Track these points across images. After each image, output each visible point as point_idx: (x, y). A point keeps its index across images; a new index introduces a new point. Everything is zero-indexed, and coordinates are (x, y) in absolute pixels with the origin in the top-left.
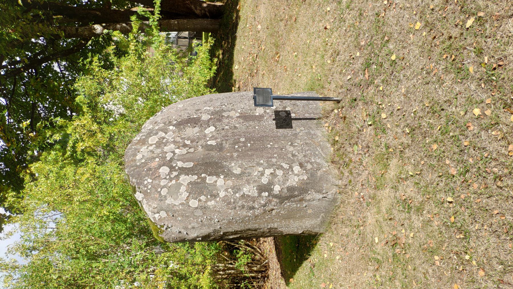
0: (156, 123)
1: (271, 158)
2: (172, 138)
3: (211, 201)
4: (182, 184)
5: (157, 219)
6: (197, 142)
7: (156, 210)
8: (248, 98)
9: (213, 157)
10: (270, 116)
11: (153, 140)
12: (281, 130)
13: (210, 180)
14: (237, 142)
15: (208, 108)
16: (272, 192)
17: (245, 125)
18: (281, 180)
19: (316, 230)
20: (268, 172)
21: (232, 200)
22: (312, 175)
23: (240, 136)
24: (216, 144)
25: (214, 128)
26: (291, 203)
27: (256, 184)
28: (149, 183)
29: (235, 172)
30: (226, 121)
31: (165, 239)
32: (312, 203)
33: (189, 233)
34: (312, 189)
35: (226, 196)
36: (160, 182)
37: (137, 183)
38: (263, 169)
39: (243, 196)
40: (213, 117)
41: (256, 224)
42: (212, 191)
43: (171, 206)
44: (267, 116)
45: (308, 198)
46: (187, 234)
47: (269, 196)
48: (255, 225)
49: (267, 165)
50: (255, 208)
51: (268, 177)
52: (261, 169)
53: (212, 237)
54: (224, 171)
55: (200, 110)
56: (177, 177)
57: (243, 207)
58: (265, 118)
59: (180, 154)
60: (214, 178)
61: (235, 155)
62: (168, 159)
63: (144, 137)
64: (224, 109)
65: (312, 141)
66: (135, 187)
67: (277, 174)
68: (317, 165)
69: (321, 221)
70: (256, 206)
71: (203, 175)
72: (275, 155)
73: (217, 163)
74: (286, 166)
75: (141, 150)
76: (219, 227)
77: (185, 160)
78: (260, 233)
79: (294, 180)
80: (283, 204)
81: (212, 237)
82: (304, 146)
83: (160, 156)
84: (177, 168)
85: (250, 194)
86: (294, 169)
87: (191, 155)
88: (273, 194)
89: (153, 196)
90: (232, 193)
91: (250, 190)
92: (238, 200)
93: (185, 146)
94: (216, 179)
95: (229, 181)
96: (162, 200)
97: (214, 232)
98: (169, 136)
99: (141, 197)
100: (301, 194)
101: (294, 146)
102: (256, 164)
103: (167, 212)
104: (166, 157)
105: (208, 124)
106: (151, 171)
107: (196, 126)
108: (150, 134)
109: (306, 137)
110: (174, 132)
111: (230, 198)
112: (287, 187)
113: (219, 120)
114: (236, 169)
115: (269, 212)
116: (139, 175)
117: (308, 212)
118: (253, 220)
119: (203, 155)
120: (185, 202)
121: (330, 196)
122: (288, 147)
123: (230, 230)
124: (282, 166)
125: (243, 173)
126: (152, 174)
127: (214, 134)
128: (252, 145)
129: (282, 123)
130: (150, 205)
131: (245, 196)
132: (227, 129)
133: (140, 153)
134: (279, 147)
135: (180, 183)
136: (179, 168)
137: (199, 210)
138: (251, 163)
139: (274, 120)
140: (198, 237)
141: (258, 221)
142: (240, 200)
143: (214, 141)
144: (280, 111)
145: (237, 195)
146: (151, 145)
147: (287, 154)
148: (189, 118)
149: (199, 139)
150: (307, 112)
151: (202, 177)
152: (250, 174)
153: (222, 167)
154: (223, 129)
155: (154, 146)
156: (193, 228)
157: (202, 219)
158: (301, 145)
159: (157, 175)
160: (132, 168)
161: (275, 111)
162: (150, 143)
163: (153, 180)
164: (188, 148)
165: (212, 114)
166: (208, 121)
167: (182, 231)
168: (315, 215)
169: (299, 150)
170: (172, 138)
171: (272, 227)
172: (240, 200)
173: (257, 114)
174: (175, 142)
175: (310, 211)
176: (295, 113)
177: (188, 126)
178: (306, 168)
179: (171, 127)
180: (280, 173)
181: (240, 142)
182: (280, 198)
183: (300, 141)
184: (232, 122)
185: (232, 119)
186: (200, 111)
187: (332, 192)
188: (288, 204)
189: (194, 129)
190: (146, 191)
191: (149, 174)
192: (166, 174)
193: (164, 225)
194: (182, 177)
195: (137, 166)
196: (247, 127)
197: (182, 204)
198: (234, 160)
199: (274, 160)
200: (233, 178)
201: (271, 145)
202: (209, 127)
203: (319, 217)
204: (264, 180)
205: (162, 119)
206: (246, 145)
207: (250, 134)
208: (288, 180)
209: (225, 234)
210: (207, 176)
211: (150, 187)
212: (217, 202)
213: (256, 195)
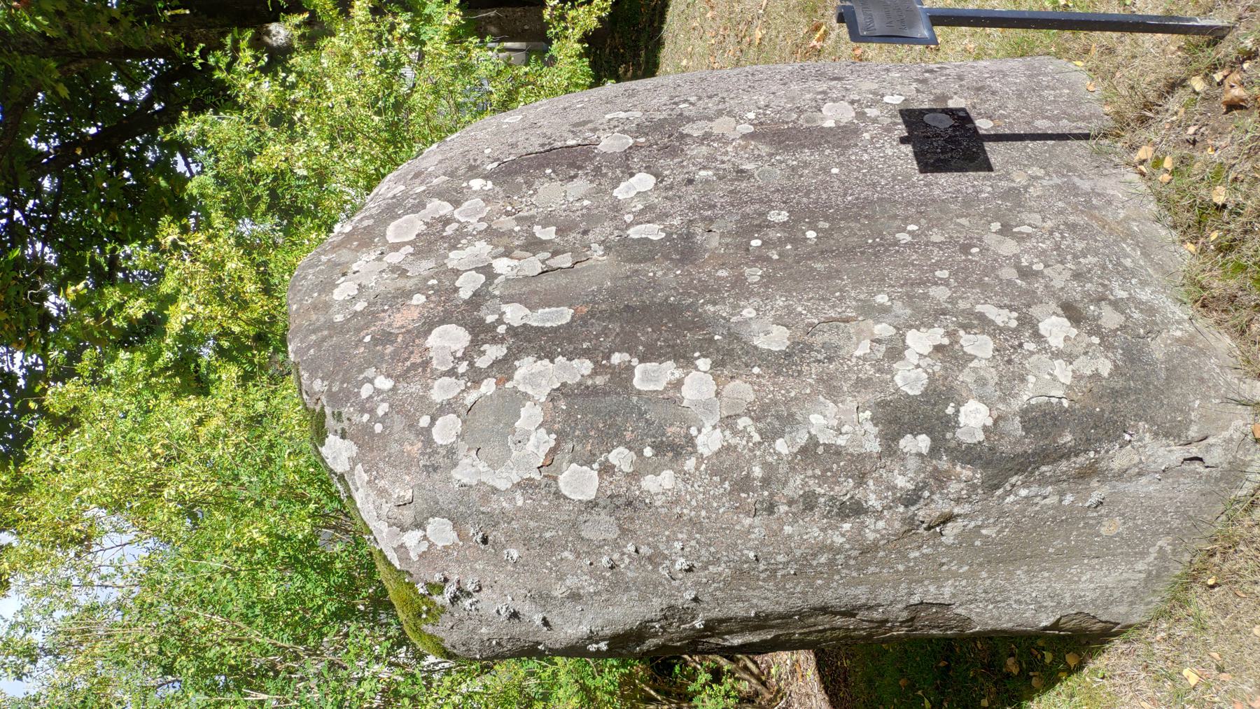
0: (417, 176)
1: (922, 283)
2: (480, 220)
3: (656, 472)
4: (526, 396)
5: (414, 556)
6: (585, 232)
7: (408, 515)
8: (778, 77)
9: (655, 284)
10: (888, 130)
11: (405, 229)
12: (945, 180)
13: (646, 377)
14: (762, 226)
15: (622, 115)
16: (949, 435)
18: (992, 376)
19: (1117, 613)
20: (920, 342)
21: (757, 472)
23: (767, 202)
24: (663, 235)
25: (651, 180)
26: (1035, 489)
27: (869, 397)
28: (378, 392)
29: (760, 342)
31: (447, 645)
32: (1130, 487)
33: (554, 619)
34: (1139, 417)
35: (727, 449)
36: (428, 388)
37: (331, 396)
38: (892, 331)
39: (809, 451)
40: (642, 140)
41: (860, 583)
42: (660, 426)
43: (474, 496)
44: (874, 129)
45: (1116, 465)
46: (546, 622)
47: (934, 451)
48: (853, 591)
49: (909, 311)
50: (866, 512)
51: (923, 363)
52: (883, 329)
53: (655, 641)
54: (711, 340)
55: (591, 121)
56: (504, 368)
57: (809, 502)
58: (867, 136)
59: (512, 275)
60: (669, 370)
61: (754, 274)
62: (465, 294)
63: (366, 223)
64: (686, 114)
65: (1092, 217)
66: (322, 415)
67: (968, 350)
68: (1141, 311)
69: (1149, 573)
70: (873, 501)
71: (617, 358)
72: (942, 274)
73: (674, 311)
74: (1001, 317)
75: (355, 267)
76: (689, 595)
77: (536, 299)
78: (865, 625)
79: (1054, 379)
80: (1000, 492)
81: (655, 641)
82: (1063, 237)
83: (432, 287)
84: (501, 329)
85: (841, 441)
86: (1043, 328)
87: (563, 280)
88: (953, 444)
89: (394, 448)
90: (757, 438)
91: (841, 424)
92: (783, 468)
93: (534, 245)
94: (678, 373)
96: (435, 469)
97: (665, 618)
98: (470, 214)
99: (345, 456)
100: (1087, 443)
101: (1021, 238)
102: (856, 309)
103: (457, 522)
104: (456, 290)
105: (624, 165)
106: (392, 342)
107: (575, 176)
108: (391, 211)
109: (1060, 204)
110: (487, 198)
111: (748, 462)
112: (1024, 413)
113: (670, 151)
114: (767, 333)
115: (929, 528)
116: (338, 362)
117: (1103, 530)
118: (846, 566)
119: (614, 278)
120: (538, 477)
121: (1216, 456)
123: (738, 610)
124: (982, 317)
126: (395, 355)
127: (654, 199)
128: (824, 235)
130: (382, 492)
131: (820, 450)
132: (707, 181)
133: (350, 275)
134: (951, 241)
135: (515, 390)
136: (510, 328)
137: (604, 516)
139: (903, 141)
140: (592, 638)
141: (871, 569)
142: (793, 469)
143: (656, 226)
144: (922, 112)
145: (781, 446)
146: (396, 247)
147: (994, 268)
148: (547, 148)
149: (591, 218)
151: (612, 367)
152: (832, 354)
153: (701, 323)
154: (690, 182)
155: (410, 249)
156: (575, 596)
157: (616, 556)
158: (1051, 233)
160: (313, 337)
161: (901, 112)
162: (391, 237)
164: (547, 255)
165: (640, 130)
166: (627, 154)
167: (525, 608)
168: (1132, 546)
169: (1044, 252)
170: (480, 220)
171: (929, 599)
172: (793, 469)
173: (829, 123)
174: (490, 234)
175: (1111, 527)
176: (990, 118)
177: (545, 176)
178: (1099, 327)
179: (476, 184)
180: (979, 346)
181: (771, 225)
182: (986, 465)
184: (726, 153)
185: (727, 144)
186: (590, 126)
187: (1226, 434)
188: (1023, 492)
189: (570, 185)
190: (367, 430)
191: (382, 355)
192: (453, 354)
193: (446, 580)
194: (526, 367)
195: (331, 326)
196: (793, 169)
197: (526, 485)
198: (752, 294)
200: (756, 370)
201: (910, 233)
202: (632, 175)
203: (1143, 554)
204: (905, 379)
205: (440, 162)
206: (799, 235)
207: (807, 194)
208: (1023, 379)
209: (712, 627)
210: (635, 361)
211: (382, 409)
212: (686, 477)
213: (873, 446)
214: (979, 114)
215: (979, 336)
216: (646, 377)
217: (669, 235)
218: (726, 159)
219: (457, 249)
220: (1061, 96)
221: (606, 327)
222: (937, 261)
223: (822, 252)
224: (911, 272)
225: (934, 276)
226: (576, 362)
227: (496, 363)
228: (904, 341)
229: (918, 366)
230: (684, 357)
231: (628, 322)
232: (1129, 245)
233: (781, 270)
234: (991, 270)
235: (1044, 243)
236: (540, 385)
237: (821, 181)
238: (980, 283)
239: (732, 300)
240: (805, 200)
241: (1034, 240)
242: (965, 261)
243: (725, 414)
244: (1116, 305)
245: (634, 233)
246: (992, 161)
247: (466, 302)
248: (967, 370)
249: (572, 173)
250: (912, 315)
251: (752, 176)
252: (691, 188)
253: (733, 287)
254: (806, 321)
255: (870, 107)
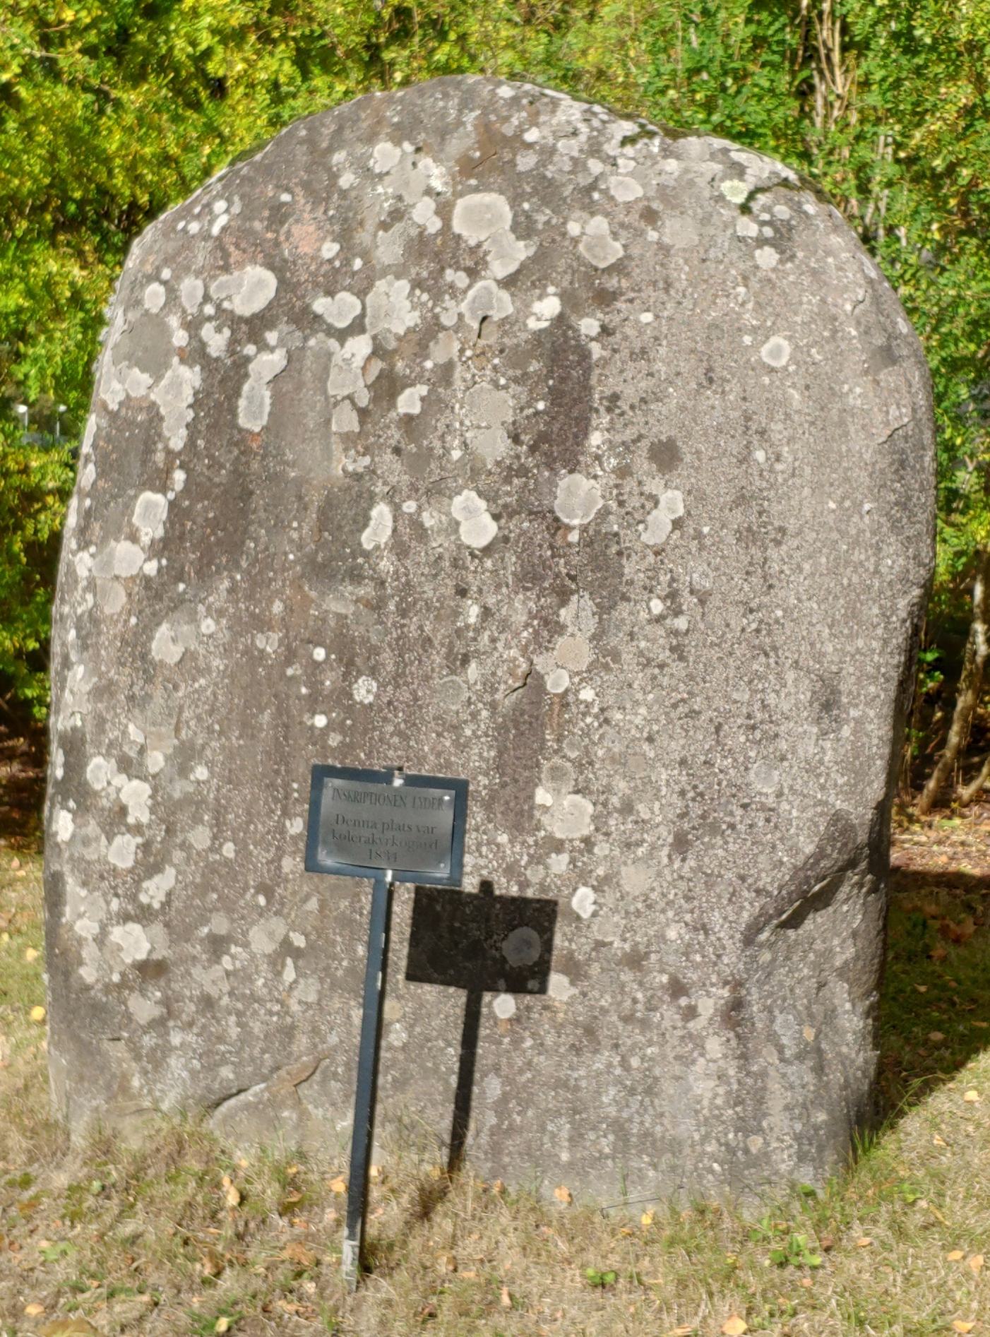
4: (158, 378)
6: (397, 451)
9: (280, 526)
17: (474, 716)
18: (90, 854)
22: (97, 1009)
29: (164, 630)
30: (520, 608)
38: (153, 770)
49: (177, 795)
51: (111, 790)
52: (156, 761)
54: (180, 578)
56: (197, 354)
59: (337, 359)
60: (151, 530)
61: (269, 643)
62: (320, 305)
67: (118, 840)
68: (153, 1050)
71: (179, 476)
72: (229, 850)
73: (234, 547)
74: (155, 890)
77: (288, 387)
79: (80, 916)
82: (271, 1013)
84: (250, 349)
86: (135, 928)
94: (145, 540)
95: (124, 599)
101: (276, 962)
104: (330, 293)
107: (516, 439)
114: (174, 640)
119: (300, 482)
122: (279, 927)
125: (146, 667)
129: (452, 930)
132: (456, 614)
135: (167, 366)
136: (248, 360)
138: (199, 719)
139: (486, 886)
143: (385, 536)
146: (444, 211)
150: (516, 1095)
153: (205, 574)
158: (282, 1003)
159: (235, 255)
163: (218, 238)
169: (250, 979)
173: (542, 796)
174: (430, 330)
176: (516, 1020)
183: (312, 998)
184: (508, 646)
192: (229, 298)
194: (191, 377)
196: (456, 728)
198: (236, 635)
199: (200, 837)
200: (133, 620)
202: (496, 517)
207: (400, 733)
208: (84, 884)
210: (171, 495)
214: (529, 1008)
215: (132, 857)
216: (149, 506)
217: (366, 555)
218: (500, 645)
219: (413, 289)
220: (554, 1144)
221: (222, 466)
222: (251, 853)
223: (286, 726)
224: (237, 816)
225: (226, 840)
226: (183, 432)
227: (203, 345)
228: (138, 777)
229: (109, 783)
230: (164, 548)
231: (225, 492)
232: (262, 1091)
233: (269, 674)
234: (228, 906)
235: (265, 985)
236: (167, 392)
237: (425, 757)
238: (205, 888)
239: (231, 610)
240: (390, 728)
241: (270, 976)
242: (246, 883)
243: (99, 582)
244: (159, 1024)
245: (381, 513)
246: (427, 987)
247: (306, 309)
248: (98, 830)
249: (525, 438)
250: (170, 797)
251: (453, 672)
252: (450, 591)
253: (252, 615)
254: (183, 686)
255: (573, 861)
